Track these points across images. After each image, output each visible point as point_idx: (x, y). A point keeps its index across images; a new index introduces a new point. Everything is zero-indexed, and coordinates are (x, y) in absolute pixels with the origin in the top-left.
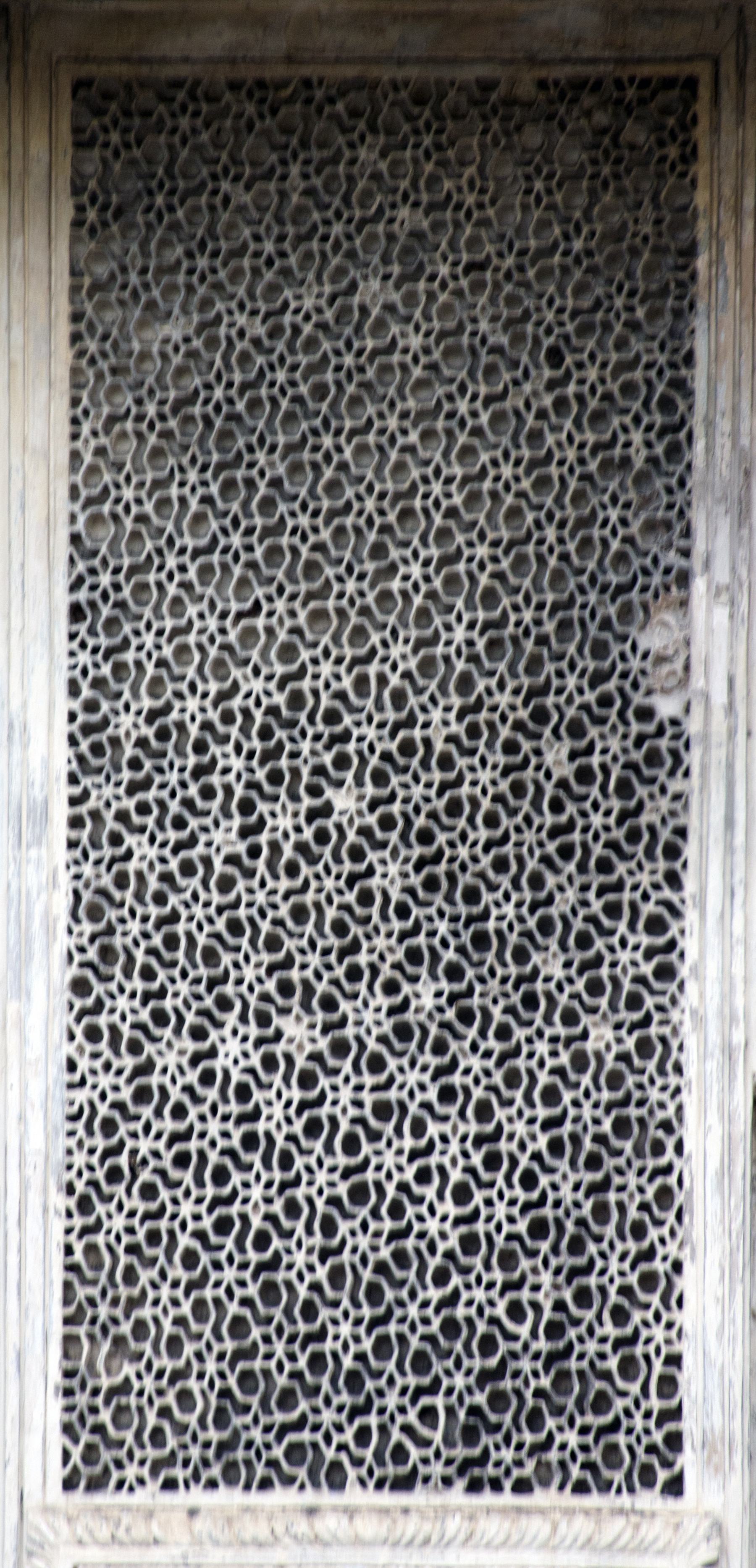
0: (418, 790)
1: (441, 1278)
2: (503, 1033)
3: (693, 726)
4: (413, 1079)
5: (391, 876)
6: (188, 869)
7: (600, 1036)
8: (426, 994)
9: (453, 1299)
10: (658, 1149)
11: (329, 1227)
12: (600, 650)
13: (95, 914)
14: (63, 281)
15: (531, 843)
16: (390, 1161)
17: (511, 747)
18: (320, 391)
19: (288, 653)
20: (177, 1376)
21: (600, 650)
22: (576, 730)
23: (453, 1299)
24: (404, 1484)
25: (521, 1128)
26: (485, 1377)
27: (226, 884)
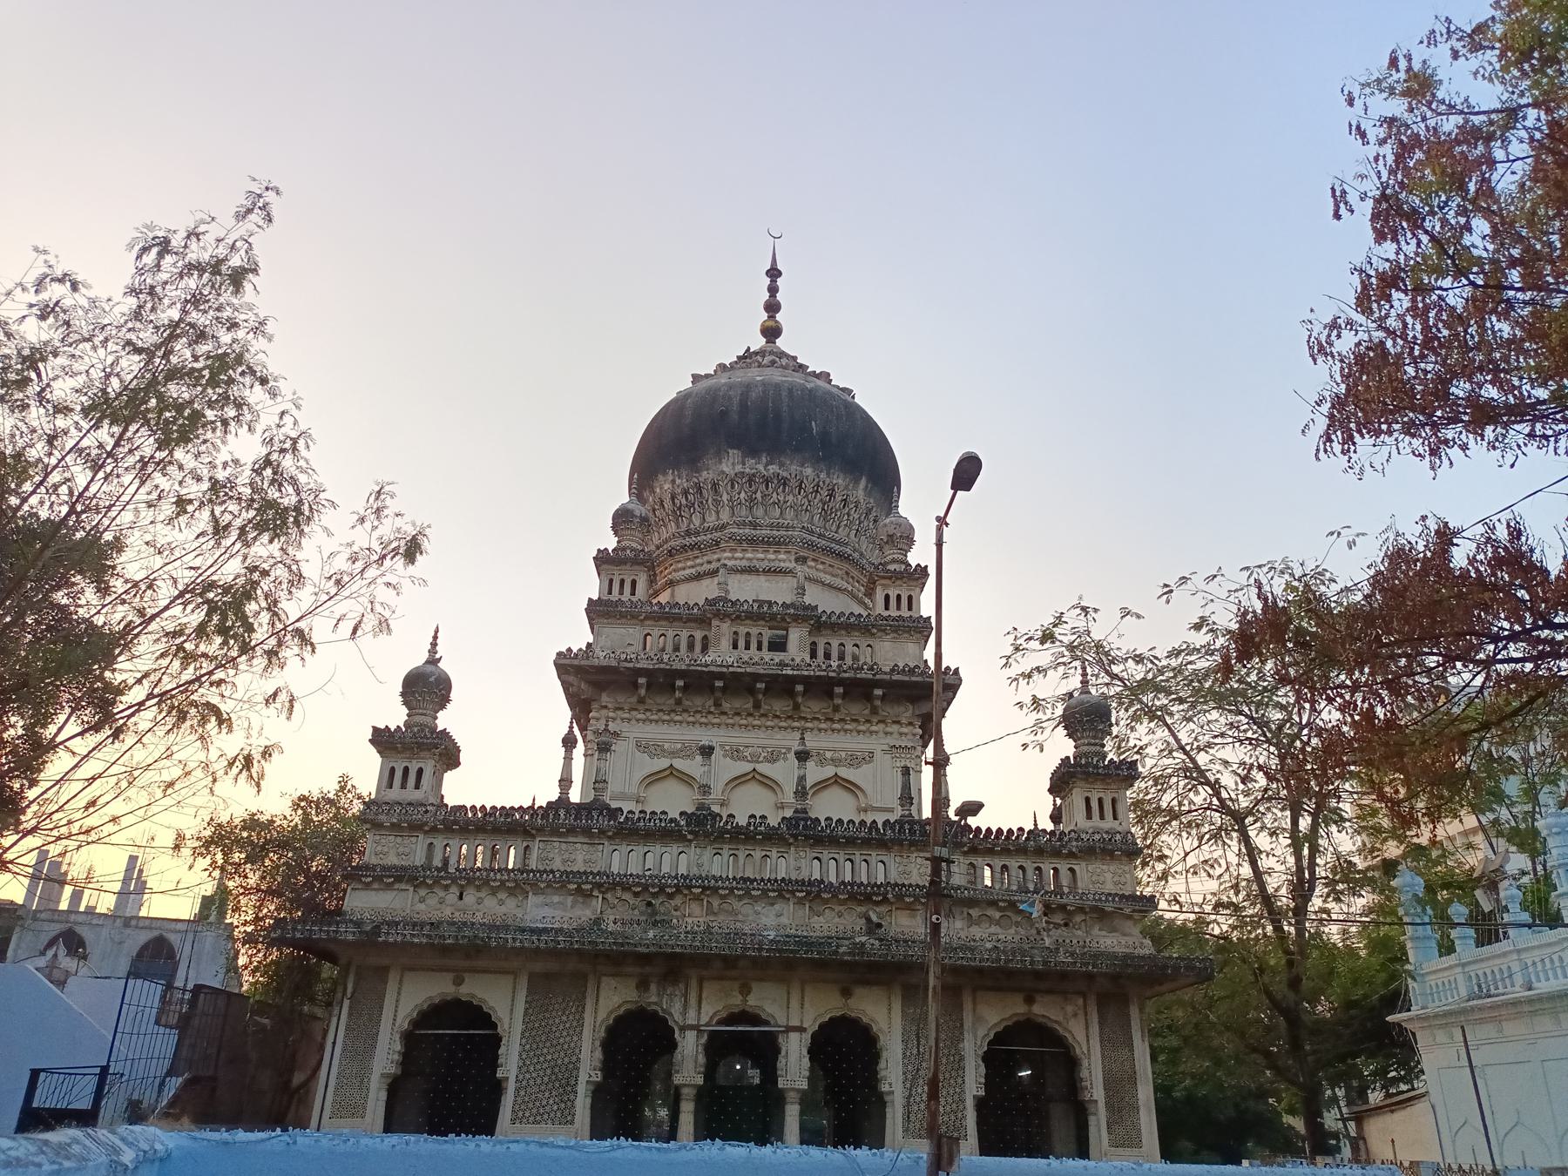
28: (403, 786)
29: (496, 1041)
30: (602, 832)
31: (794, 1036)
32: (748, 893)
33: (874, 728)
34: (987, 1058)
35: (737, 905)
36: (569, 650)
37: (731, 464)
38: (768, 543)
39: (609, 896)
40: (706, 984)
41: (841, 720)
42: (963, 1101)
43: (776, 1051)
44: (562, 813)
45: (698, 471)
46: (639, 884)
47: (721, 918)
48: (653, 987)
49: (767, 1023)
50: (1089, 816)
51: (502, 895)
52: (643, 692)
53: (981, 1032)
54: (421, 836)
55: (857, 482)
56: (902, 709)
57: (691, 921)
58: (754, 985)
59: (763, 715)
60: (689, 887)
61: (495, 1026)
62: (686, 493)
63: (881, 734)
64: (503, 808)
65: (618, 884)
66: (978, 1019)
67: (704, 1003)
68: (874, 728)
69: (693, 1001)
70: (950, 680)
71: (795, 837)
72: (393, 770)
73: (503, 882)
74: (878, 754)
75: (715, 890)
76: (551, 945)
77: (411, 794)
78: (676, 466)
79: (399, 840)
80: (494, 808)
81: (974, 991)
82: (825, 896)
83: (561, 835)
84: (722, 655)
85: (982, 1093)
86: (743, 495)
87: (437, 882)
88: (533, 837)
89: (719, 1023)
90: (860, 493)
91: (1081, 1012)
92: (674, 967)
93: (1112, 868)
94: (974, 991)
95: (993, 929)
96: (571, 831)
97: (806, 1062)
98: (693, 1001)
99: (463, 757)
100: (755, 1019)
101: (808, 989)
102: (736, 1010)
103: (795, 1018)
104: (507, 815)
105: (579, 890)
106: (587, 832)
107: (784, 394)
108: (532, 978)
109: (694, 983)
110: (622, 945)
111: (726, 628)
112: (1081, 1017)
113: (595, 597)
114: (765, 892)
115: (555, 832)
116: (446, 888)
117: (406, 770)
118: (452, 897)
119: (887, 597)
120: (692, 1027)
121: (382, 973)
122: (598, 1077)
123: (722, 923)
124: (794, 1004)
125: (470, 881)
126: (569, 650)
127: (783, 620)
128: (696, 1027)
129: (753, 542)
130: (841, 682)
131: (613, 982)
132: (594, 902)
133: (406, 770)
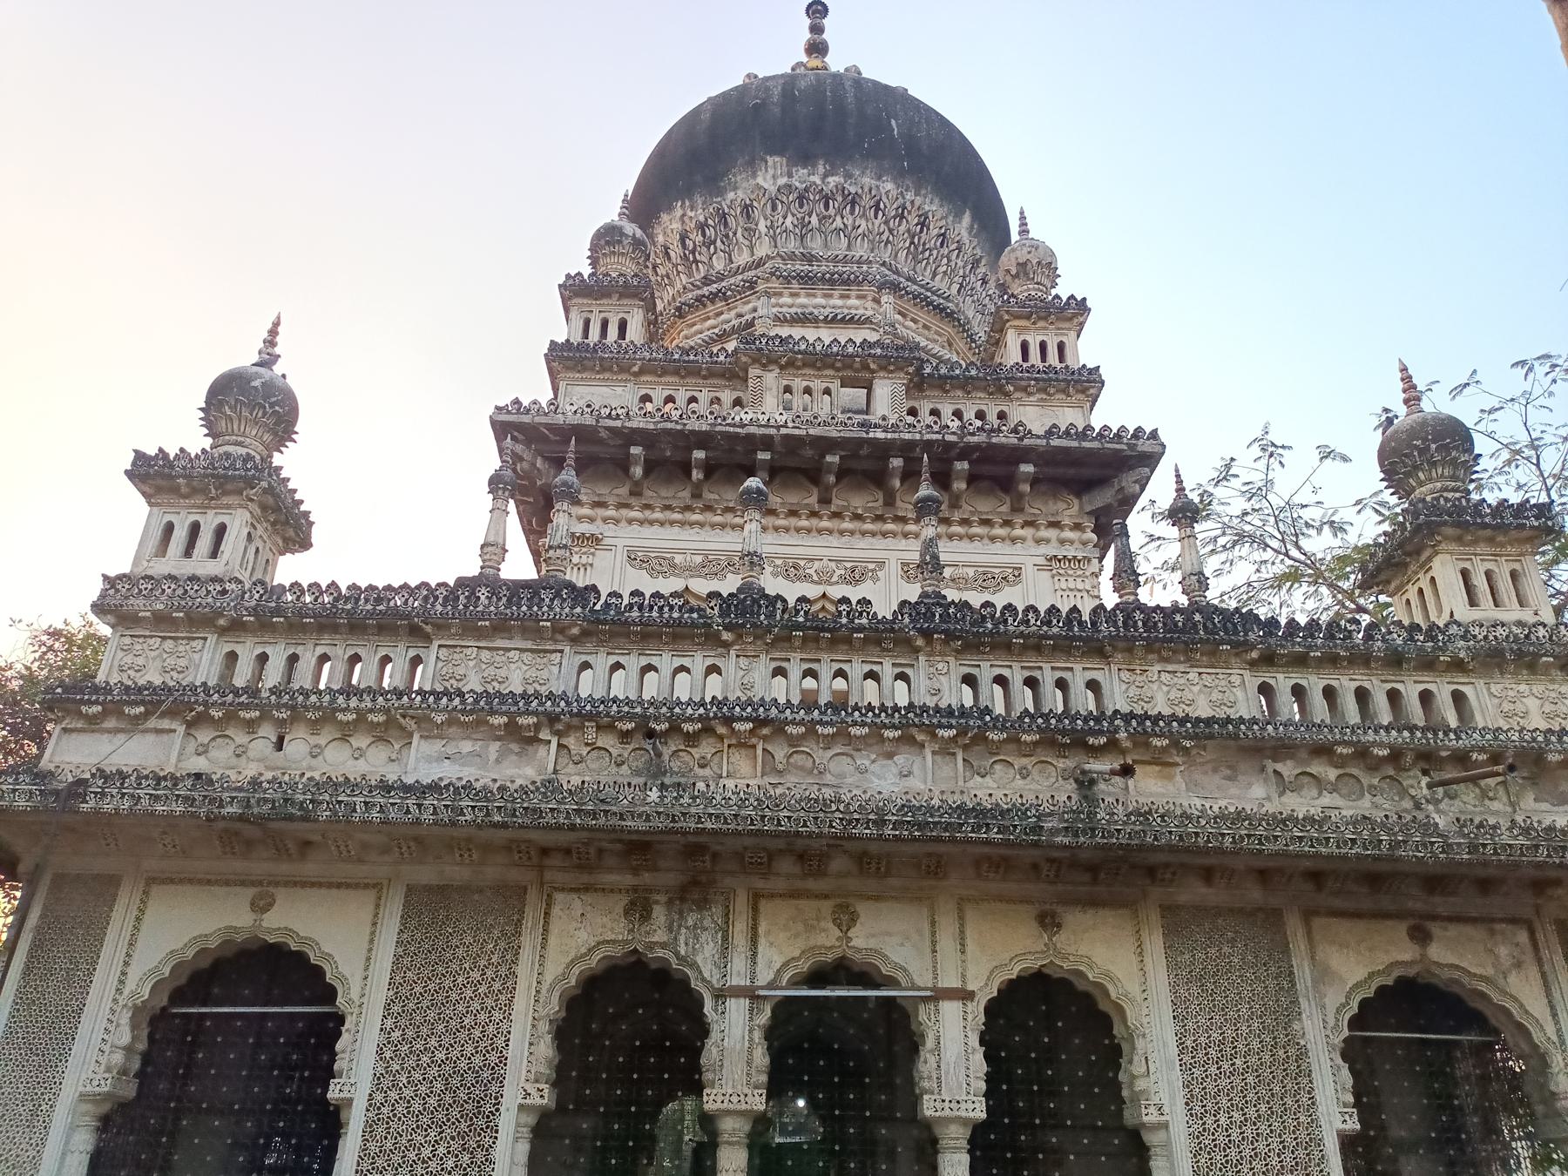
8: (1263, 1107)
15: (1280, 1074)
16: (1261, 1146)
28: (188, 552)
29: (328, 1029)
30: (559, 630)
31: (950, 1009)
32: (842, 735)
33: (1018, 532)
34: (1352, 1052)
35: (822, 756)
36: (517, 402)
37: (771, 176)
38: (832, 282)
39: (570, 741)
40: (764, 905)
41: (965, 522)
42: (1320, 1142)
43: (913, 1045)
44: (483, 594)
45: (721, 192)
46: (630, 717)
47: (790, 779)
48: (659, 914)
49: (891, 982)
50: (1473, 603)
51: (360, 741)
52: (638, 471)
53: (1334, 998)
54: (212, 639)
55: (958, 216)
56: (1061, 505)
57: (734, 780)
58: (862, 908)
59: (837, 515)
60: (728, 721)
61: (329, 995)
62: (702, 227)
63: (1030, 542)
64: (371, 588)
65: (590, 717)
66: (1323, 975)
67: (762, 942)
68: (1018, 532)
69: (740, 929)
70: (1145, 446)
71: (927, 634)
72: (169, 529)
73: (361, 715)
74: (1029, 572)
75: (779, 728)
76: (445, 816)
77: (201, 564)
78: (687, 193)
79: (169, 644)
80: (353, 587)
81: (1308, 915)
82: (993, 736)
83: (480, 634)
84: (770, 407)
85: (1353, 1125)
86: (789, 219)
87: (231, 717)
88: (428, 639)
89: (795, 983)
90: (963, 228)
91: (1529, 957)
92: (703, 864)
93: (1538, 689)
94: (1308, 915)
95: (1327, 799)
96: (501, 627)
97: (979, 1064)
98: (740, 929)
99: (316, 535)
100: (865, 977)
101: (970, 915)
102: (830, 957)
103: (949, 973)
104: (379, 600)
105: (513, 731)
106: (530, 629)
107: (848, 84)
108: (410, 890)
109: (741, 903)
110: (594, 815)
111: (772, 379)
112: (1533, 972)
113: (561, 339)
114: (877, 728)
115: (471, 628)
116: (251, 726)
117: (195, 529)
118: (261, 745)
119: (1025, 347)
120: (738, 992)
121: (106, 887)
122: (543, 1097)
123: (796, 785)
124: (947, 943)
125: (297, 714)
126: (517, 402)
127: (866, 367)
128: (751, 994)
129: (806, 280)
130: (966, 452)
131: (577, 903)
132: (542, 751)
133: (195, 529)
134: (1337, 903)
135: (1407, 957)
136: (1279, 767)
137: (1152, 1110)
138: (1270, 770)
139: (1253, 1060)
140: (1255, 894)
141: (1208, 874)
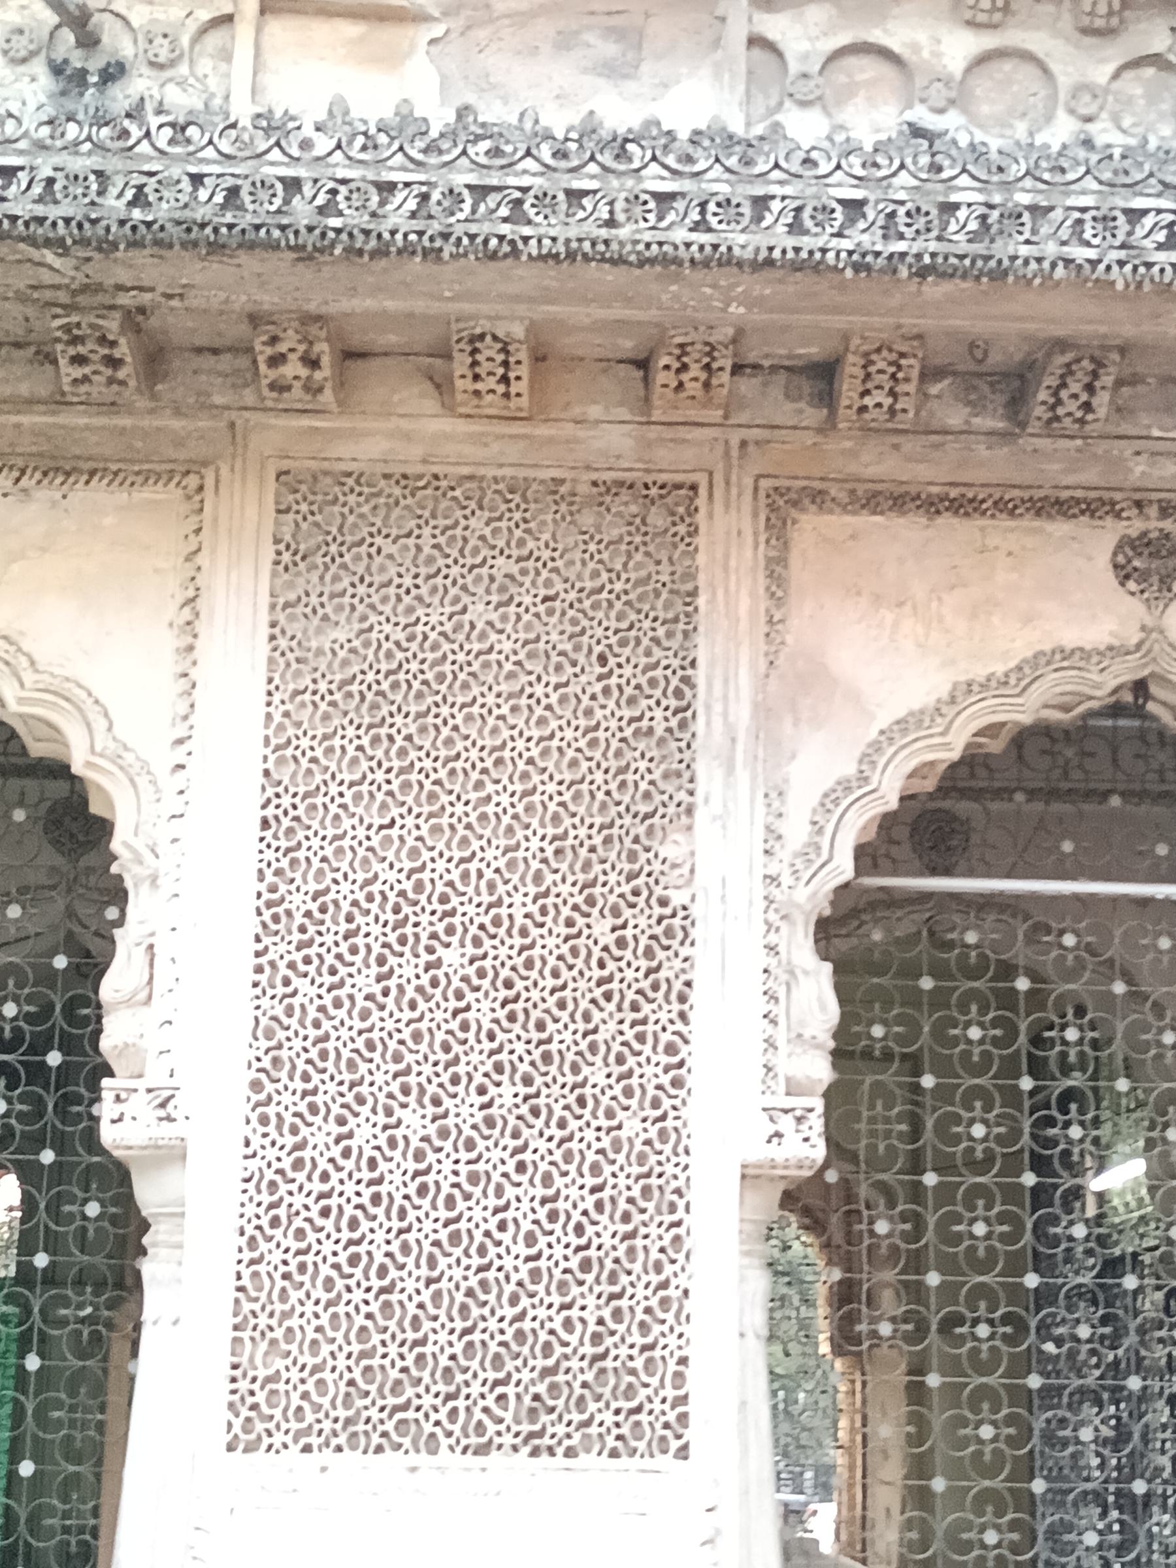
0: (503, 951)
1: (514, 1300)
2: (562, 1124)
3: (695, 911)
4: (496, 1156)
5: (483, 1011)
6: (338, 1004)
7: (631, 1127)
8: (507, 1094)
9: (521, 1317)
10: (673, 1208)
11: (432, 1263)
12: (632, 857)
13: (269, 1034)
14: (264, 600)
15: (584, 990)
17: (570, 923)
18: (441, 678)
19: (414, 853)
20: (316, 1369)
21: (632, 857)
22: (616, 912)
23: (521, 1317)
24: (482, 1450)
25: (574, 1195)
26: (546, 1372)
27: (365, 1015)
42: (675, 1202)
53: (819, 761)
66: (796, 688)
81: (784, 506)
94: (782, 506)
134: (880, 464)
135: (1096, 632)
136: (774, 26)
137: (140, 1106)
138: (737, 33)
139: (503, 951)
140: (607, 436)
141: (444, 360)
